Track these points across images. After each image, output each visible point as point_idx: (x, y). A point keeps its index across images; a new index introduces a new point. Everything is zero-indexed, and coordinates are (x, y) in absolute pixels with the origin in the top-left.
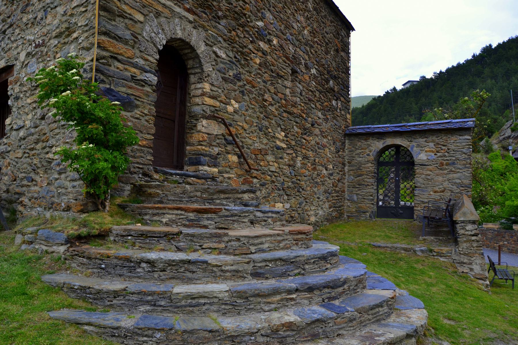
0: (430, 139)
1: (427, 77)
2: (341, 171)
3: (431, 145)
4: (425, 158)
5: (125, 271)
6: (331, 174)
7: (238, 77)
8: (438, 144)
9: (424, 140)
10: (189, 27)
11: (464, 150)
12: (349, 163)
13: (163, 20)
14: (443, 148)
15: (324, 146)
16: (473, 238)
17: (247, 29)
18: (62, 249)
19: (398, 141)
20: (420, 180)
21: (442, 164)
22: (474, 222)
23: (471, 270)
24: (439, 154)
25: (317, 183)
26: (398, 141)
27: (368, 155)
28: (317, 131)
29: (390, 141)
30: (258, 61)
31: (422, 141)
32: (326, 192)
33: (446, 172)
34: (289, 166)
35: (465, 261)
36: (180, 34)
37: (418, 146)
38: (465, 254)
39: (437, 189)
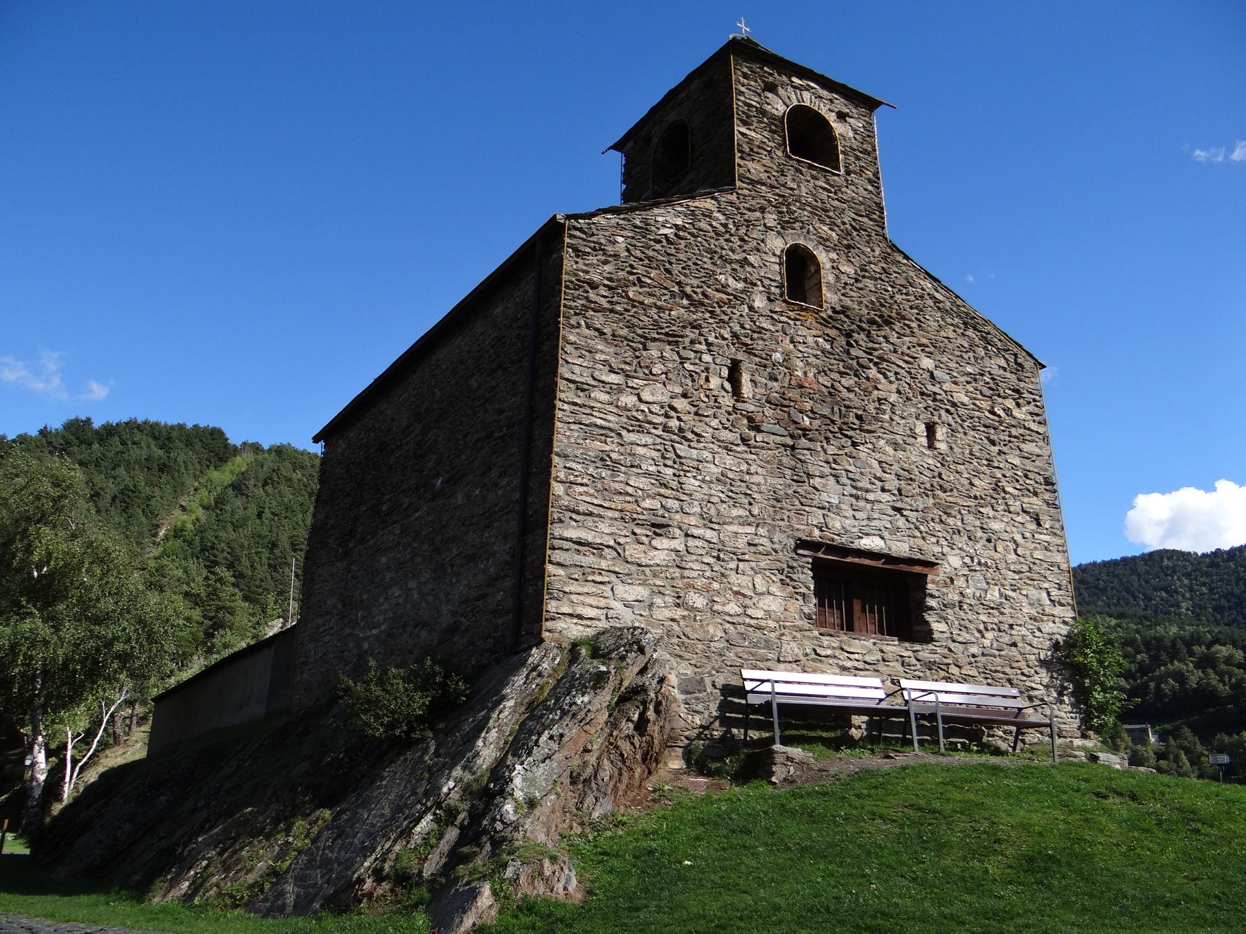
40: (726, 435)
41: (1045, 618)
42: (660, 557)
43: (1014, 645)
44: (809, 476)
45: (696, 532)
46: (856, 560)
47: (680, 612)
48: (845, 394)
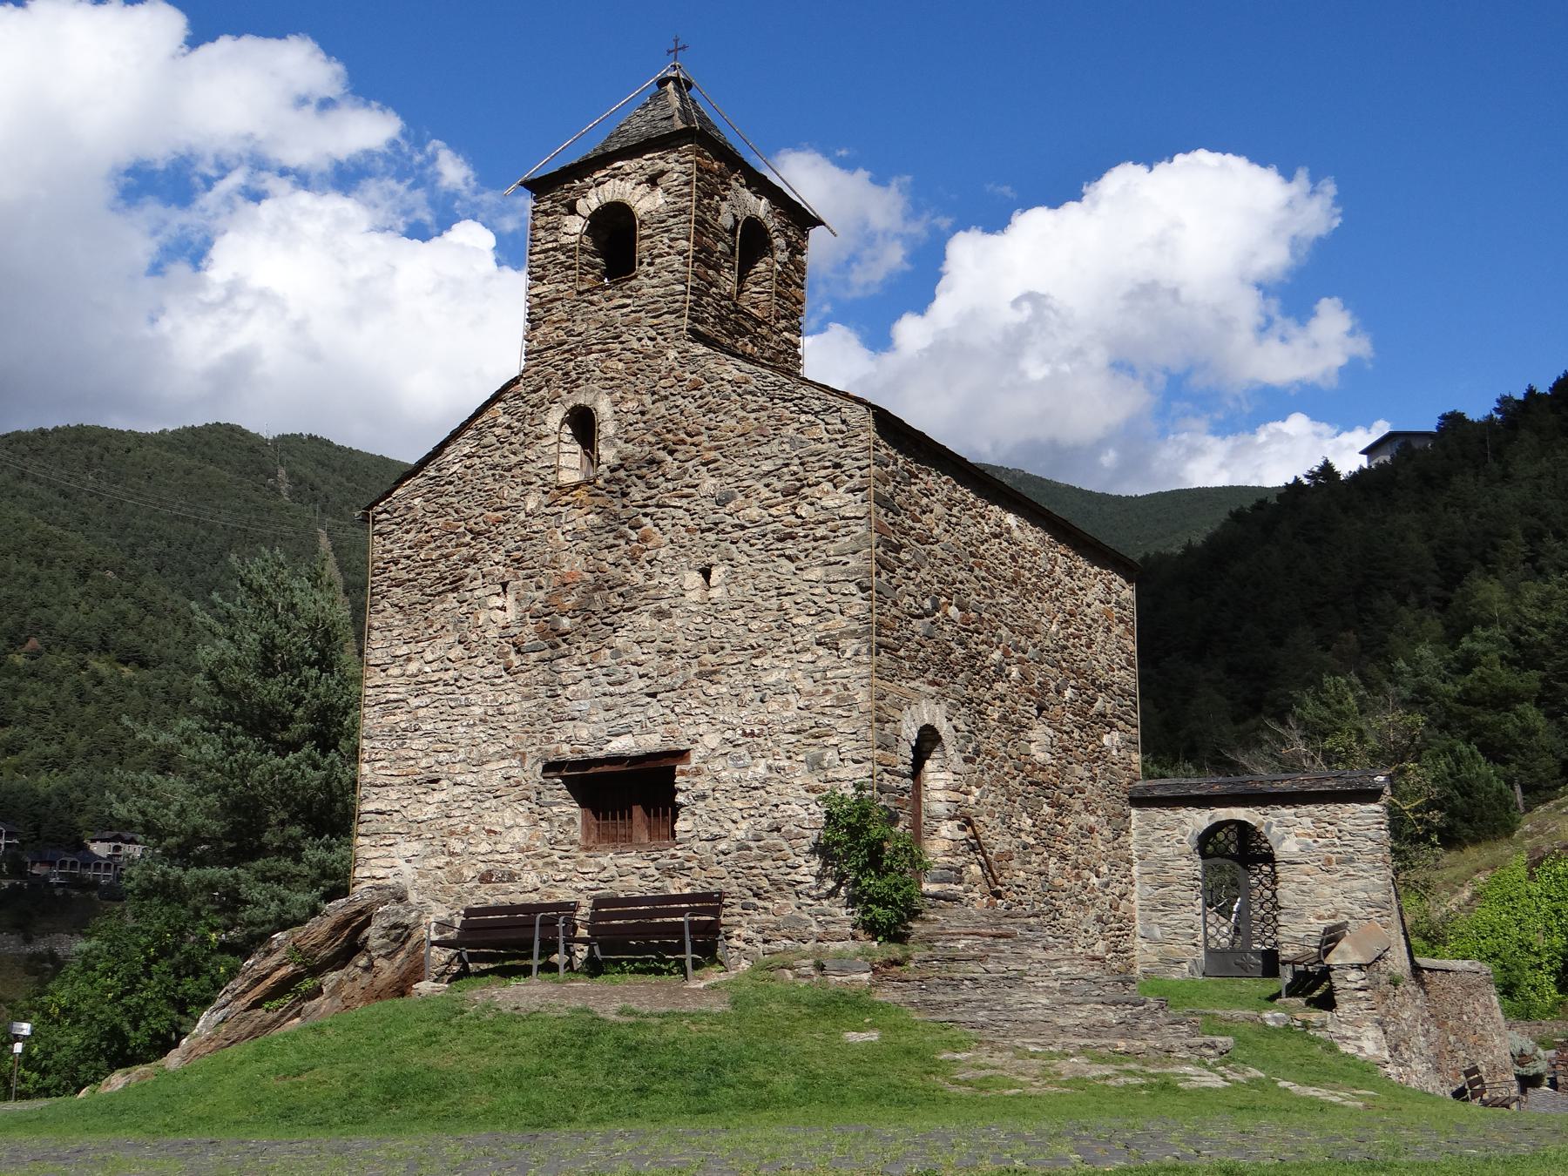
0: (1303, 809)
1: (1470, 416)
4: (1295, 849)
5: (949, 989)
6: (1107, 885)
7: (977, 752)
8: (1320, 821)
9: (1293, 810)
11: (1370, 834)
12: (1140, 858)
13: (913, 707)
14: (1330, 828)
15: (1092, 830)
18: (865, 976)
20: (1287, 893)
21: (1329, 861)
22: (1360, 967)
23: (1361, 1049)
25: (1082, 902)
27: (1180, 842)
28: (1077, 805)
30: (996, 716)
31: (1287, 812)
32: (1099, 919)
33: (1337, 876)
34: (1041, 874)
35: (1350, 1034)
38: (1348, 1023)
40: (489, 671)
42: (430, 811)
44: (565, 686)
45: (459, 779)
46: (600, 769)
48: (612, 571)
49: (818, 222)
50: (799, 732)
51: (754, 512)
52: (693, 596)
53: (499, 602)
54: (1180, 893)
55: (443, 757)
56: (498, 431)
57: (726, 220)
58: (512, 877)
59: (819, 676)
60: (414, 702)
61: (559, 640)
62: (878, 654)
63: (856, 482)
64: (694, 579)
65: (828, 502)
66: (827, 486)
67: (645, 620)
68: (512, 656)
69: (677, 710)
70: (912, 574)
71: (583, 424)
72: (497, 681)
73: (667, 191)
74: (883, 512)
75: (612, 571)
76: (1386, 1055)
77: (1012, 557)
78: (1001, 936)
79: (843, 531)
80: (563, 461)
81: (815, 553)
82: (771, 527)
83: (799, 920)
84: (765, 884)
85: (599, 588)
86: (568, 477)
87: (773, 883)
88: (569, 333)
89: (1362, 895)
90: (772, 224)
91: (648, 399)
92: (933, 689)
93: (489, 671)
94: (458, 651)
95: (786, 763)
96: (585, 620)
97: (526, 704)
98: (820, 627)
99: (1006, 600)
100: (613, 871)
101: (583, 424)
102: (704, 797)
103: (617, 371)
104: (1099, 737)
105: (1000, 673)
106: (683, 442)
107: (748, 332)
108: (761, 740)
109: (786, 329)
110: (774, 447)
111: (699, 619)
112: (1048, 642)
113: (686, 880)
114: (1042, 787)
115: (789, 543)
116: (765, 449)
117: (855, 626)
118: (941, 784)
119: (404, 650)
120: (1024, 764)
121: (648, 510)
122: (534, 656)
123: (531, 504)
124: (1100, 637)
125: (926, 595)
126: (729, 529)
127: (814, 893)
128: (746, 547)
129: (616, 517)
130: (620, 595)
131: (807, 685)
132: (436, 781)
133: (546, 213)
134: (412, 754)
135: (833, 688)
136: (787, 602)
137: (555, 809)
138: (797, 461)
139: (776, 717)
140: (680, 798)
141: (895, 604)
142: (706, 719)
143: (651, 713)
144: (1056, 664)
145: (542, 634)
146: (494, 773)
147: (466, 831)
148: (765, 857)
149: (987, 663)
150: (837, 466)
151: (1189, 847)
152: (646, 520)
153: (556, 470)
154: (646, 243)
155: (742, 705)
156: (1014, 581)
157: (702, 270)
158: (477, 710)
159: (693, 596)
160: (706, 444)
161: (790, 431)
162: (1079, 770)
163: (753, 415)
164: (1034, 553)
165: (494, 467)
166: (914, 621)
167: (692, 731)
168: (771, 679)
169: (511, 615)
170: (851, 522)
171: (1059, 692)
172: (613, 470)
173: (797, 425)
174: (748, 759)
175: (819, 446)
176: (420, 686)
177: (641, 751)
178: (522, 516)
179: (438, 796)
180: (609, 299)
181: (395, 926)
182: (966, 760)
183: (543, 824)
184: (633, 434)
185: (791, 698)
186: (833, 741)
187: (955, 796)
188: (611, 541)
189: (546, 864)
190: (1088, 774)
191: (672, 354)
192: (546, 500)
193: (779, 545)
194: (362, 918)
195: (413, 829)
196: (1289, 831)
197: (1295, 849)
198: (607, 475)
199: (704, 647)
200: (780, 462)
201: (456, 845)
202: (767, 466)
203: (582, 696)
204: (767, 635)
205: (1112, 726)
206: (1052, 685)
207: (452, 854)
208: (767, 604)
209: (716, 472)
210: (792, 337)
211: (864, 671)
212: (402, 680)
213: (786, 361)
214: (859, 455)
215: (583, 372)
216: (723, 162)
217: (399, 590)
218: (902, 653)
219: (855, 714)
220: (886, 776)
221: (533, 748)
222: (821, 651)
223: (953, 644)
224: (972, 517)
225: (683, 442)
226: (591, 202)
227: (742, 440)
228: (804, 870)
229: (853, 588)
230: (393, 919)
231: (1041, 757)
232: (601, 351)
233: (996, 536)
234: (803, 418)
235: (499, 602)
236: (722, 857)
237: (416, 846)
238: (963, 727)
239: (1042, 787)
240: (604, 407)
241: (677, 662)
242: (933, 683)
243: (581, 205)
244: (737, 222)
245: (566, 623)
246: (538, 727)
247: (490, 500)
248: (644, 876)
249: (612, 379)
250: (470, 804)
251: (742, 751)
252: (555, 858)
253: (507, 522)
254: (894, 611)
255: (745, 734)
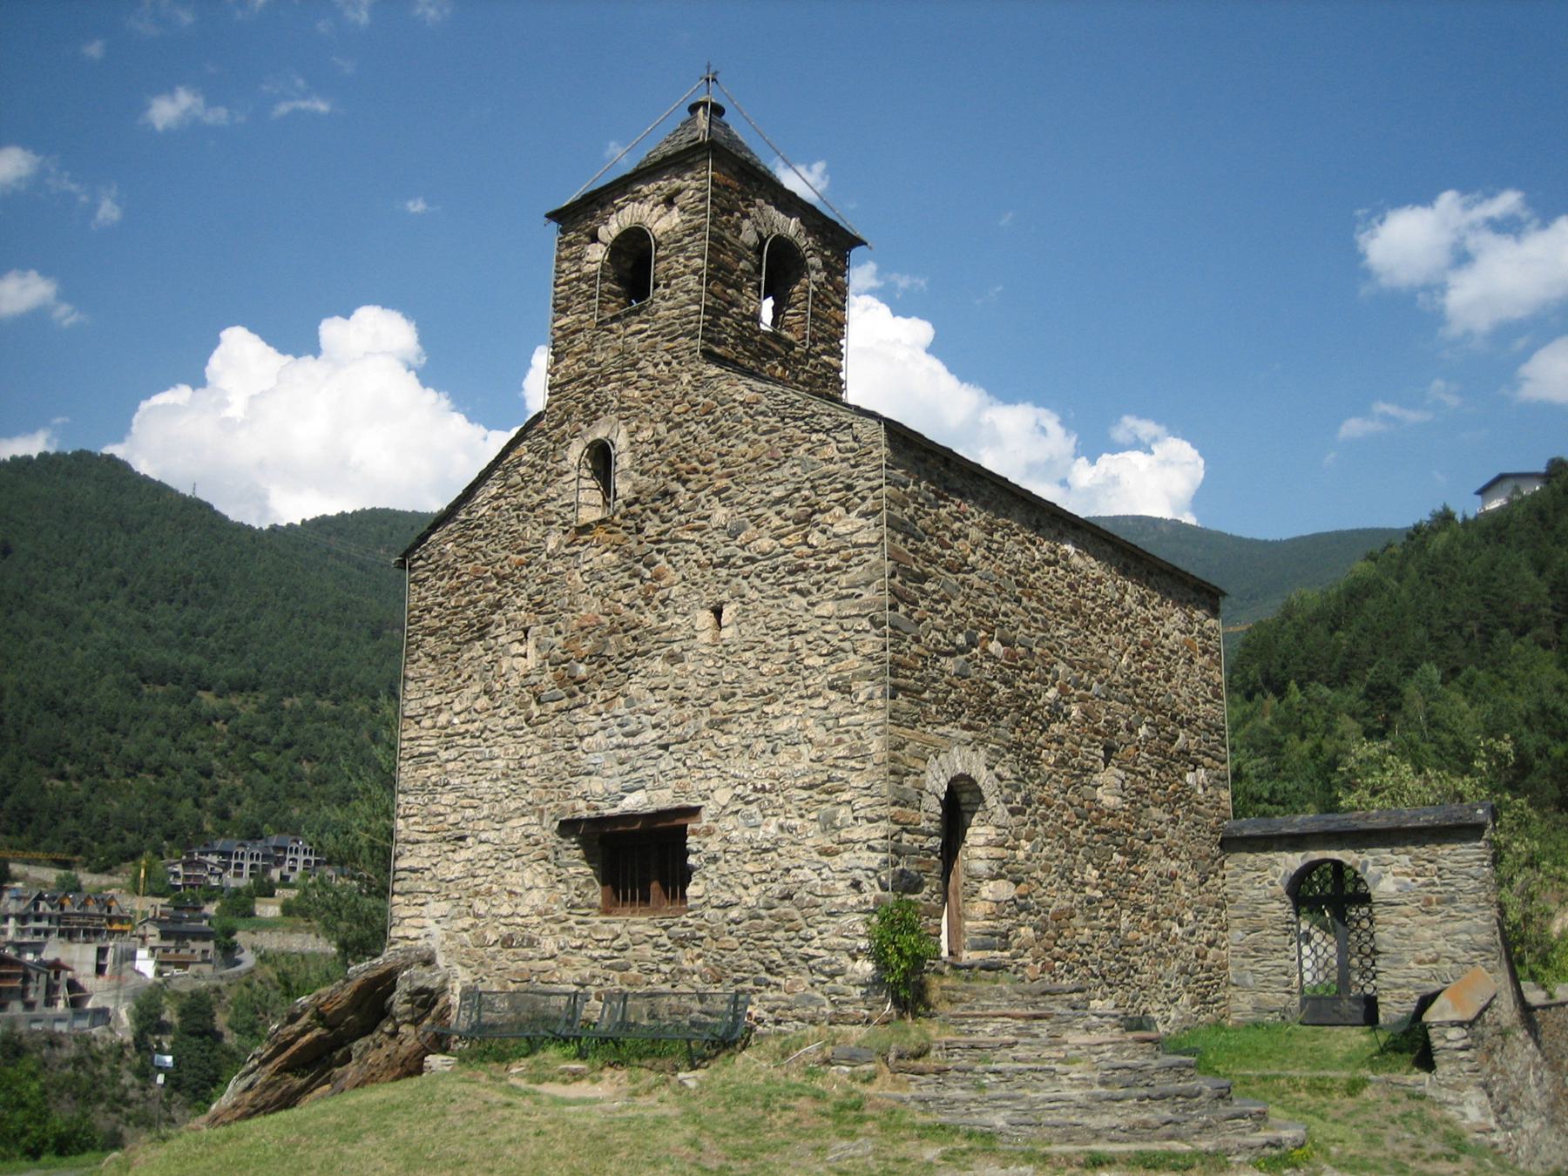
2: (1214, 922)
3: (1405, 859)
4: (1393, 889)
6: (1192, 933)
7: (1027, 801)
10: (967, 751)
11: (1472, 871)
13: (942, 757)
14: (1429, 866)
15: (1173, 876)
16: (1462, 1054)
17: (1035, 713)
19: (1335, 855)
20: (1385, 935)
21: (1429, 902)
22: (1460, 1024)
23: (1464, 1115)
24: (1420, 880)
25: (1162, 955)
26: (1335, 855)
27: (1272, 883)
28: (1156, 851)
29: (1316, 855)
30: (1052, 760)
31: (1384, 853)
32: (1183, 971)
33: (1437, 918)
34: (1110, 929)
35: (1451, 1098)
36: (960, 769)
37: (1377, 862)
38: (1448, 1086)
39: (1422, 955)
41: (841, 848)
42: (457, 870)
43: (789, 897)
45: (483, 836)
47: (468, 921)
48: (626, 612)
49: (861, 243)
50: (811, 787)
51: (766, 543)
52: (705, 637)
53: (517, 648)
54: (1273, 939)
55: (469, 812)
56: (522, 470)
57: (749, 236)
58: (531, 943)
59: (830, 722)
60: (444, 755)
61: (576, 688)
62: (893, 697)
63: (868, 505)
64: (705, 618)
65: (839, 528)
66: (839, 510)
67: (658, 665)
68: (533, 706)
69: (689, 762)
70: (941, 606)
71: (601, 458)
72: (519, 733)
73: (682, 209)
74: (900, 537)
75: (626, 612)
76: (1492, 1122)
77: (1071, 586)
78: (1036, 1017)
79: (855, 560)
80: (582, 497)
81: (827, 586)
82: (781, 559)
83: (811, 1000)
84: (776, 957)
85: (613, 632)
86: (588, 515)
87: (786, 956)
88: (590, 364)
89: (1464, 937)
90: (805, 242)
91: (662, 428)
92: (968, 735)
93: (511, 722)
94: (483, 701)
95: (797, 822)
96: (601, 666)
97: (546, 757)
98: (832, 668)
99: (1063, 632)
100: (625, 939)
101: (601, 458)
102: (715, 859)
103: (633, 399)
104: (1181, 776)
105: (1057, 712)
106: (695, 470)
107: (777, 354)
108: (772, 796)
109: (824, 352)
110: (786, 471)
111: (711, 663)
112: (1117, 677)
113: (697, 951)
114: (1115, 836)
115: (801, 577)
116: (775, 474)
117: (872, 667)
118: (982, 840)
119: (434, 701)
120: (1089, 813)
121: (663, 546)
122: (552, 706)
123: (551, 544)
124: (1181, 670)
125: (958, 630)
126: (740, 563)
127: (827, 968)
128: (757, 582)
129: (631, 554)
130: (635, 639)
131: (818, 734)
132: (463, 838)
133: (570, 244)
134: (441, 809)
135: (845, 737)
136: (798, 641)
137: (572, 870)
138: (808, 485)
139: (787, 770)
140: (692, 860)
141: (917, 640)
142: (716, 773)
143: (662, 766)
144: (1128, 700)
145: (561, 682)
146: (516, 829)
147: (489, 892)
148: (776, 928)
149: (1040, 703)
150: (849, 488)
151: (1281, 889)
152: (661, 558)
153: (574, 506)
154: (663, 265)
155: (754, 758)
156: (1073, 612)
157: (718, 289)
158: (500, 763)
159: (705, 637)
160: (718, 472)
161: (800, 452)
162: (1156, 813)
163: (764, 438)
164: (1098, 581)
165: (519, 507)
166: (943, 660)
167: (703, 785)
168: (781, 726)
169: (532, 662)
170: (864, 550)
171: (1131, 729)
172: (629, 505)
173: (808, 445)
174: (759, 818)
175: (831, 467)
176: (448, 738)
177: (651, 809)
178: (543, 558)
179: (464, 854)
180: (627, 326)
181: (421, 991)
182: (1013, 812)
183: (561, 886)
184: (648, 466)
185: (803, 748)
186: (845, 796)
187: (998, 852)
188: (626, 581)
189: (563, 929)
190: (1167, 816)
191: (686, 377)
192: (566, 539)
193: (791, 579)
194: (387, 981)
195: (443, 887)
196: (1387, 873)
197: (1393, 889)
198: (623, 509)
199: (715, 694)
200: (790, 486)
201: (480, 906)
202: (778, 492)
203: (597, 748)
204: (779, 679)
205: (1197, 765)
206: (1123, 722)
207: (477, 916)
208: (778, 645)
209: (727, 501)
210: (833, 361)
211: (878, 717)
212: (432, 732)
213: (828, 385)
214: (872, 475)
215: (603, 403)
216: (746, 179)
217: (432, 639)
218: (926, 695)
219: (869, 766)
220: (906, 836)
221: (551, 805)
222: (833, 695)
223: (995, 684)
224: (1019, 543)
225: (695, 470)
226: (611, 229)
227: (753, 465)
228: (817, 942)
229: (866, 624)
230: (419, 984)
231: (1109, 800)
232: (618, 380)
233: (1048, 563)
234: (814, 437)
235: (522, 650)
236: (733, 927)
237: (445, 907)
238: (1008, 774)
239: (1115, 836)
240: (621, 441)
241: (688, 711)
242: (965, 727)
243: (602, 231)
244: (763, 241)
245: (582, 670)
246: (557, 782)
247: (513, 542)
248: (656, 946)
249: (629, 408)
250: (492, 863)
251: (754, 808)
252: (571, 923)
253: (529, 565)
254: (915, 648)
255: (755, 789)
